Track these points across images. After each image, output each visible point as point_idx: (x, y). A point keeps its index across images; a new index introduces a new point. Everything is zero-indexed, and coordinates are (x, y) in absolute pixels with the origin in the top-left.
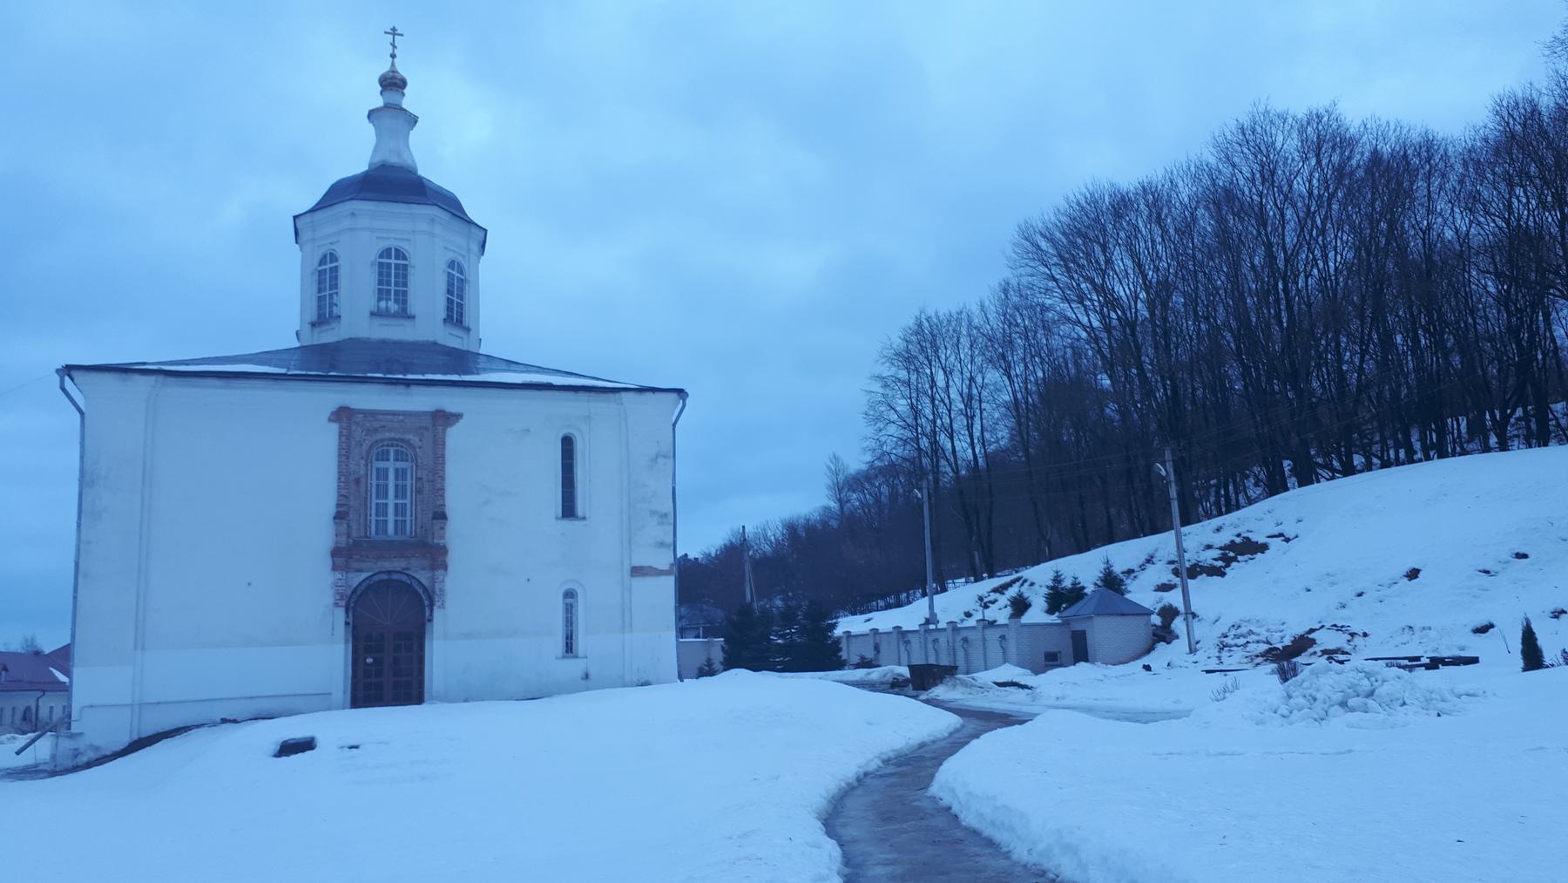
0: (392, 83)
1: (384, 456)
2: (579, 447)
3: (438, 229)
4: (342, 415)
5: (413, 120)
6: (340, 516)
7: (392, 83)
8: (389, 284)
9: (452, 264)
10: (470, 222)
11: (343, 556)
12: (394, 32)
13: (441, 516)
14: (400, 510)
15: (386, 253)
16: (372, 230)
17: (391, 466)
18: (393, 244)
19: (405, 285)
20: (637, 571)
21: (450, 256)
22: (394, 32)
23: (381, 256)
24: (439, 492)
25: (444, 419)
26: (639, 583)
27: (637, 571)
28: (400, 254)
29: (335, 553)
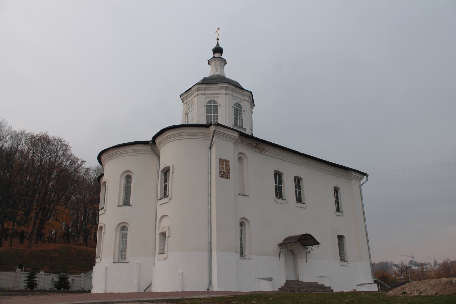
0: (218, 50)
3: (229, 92)
5: (225, 62)
7: (218, 50)
8: (211, 113)
9: (236, 104)
10: (243, 89)
16: (205, 94)
19: (217, 113)
21: (235, 102)
23: (208, 103)
28: (214, 102)
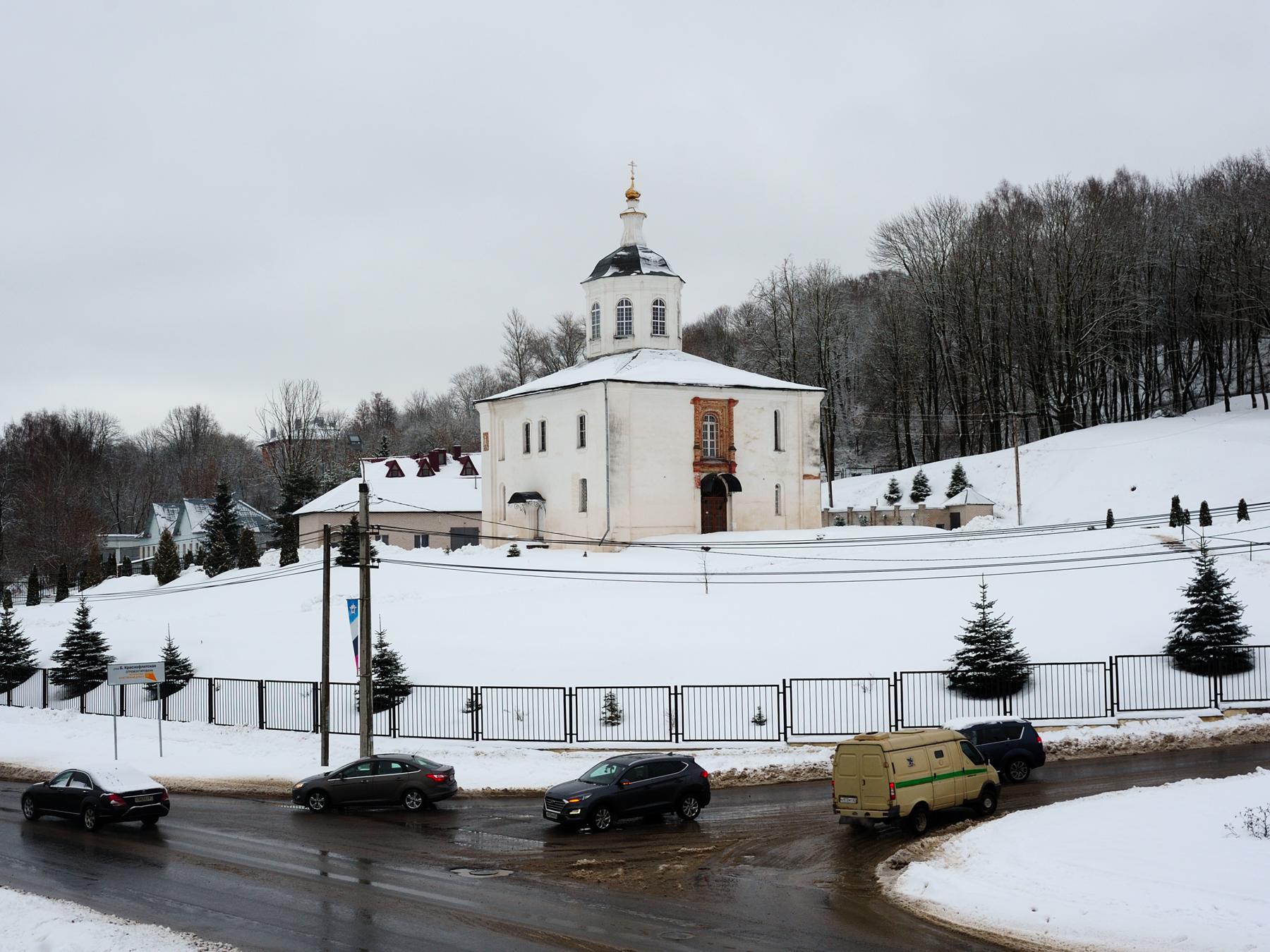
0: (632, 197)
1: (706, 419)
2: (781, 417)
4: (696, 400)
6: (696, 447)
7: (632, 197)
11: (698, 464)
12: (632, 164)
13: (732, 449)
14: (712, 443)
15: (656, 303)
17: (709, 423)
18: (658, 297)
20: (806, 477)
22: (632, 164)
24: (731, 437)
25: (732, 402)
26: (808, 482)
27: (806, 477)
29: (695, 464)
